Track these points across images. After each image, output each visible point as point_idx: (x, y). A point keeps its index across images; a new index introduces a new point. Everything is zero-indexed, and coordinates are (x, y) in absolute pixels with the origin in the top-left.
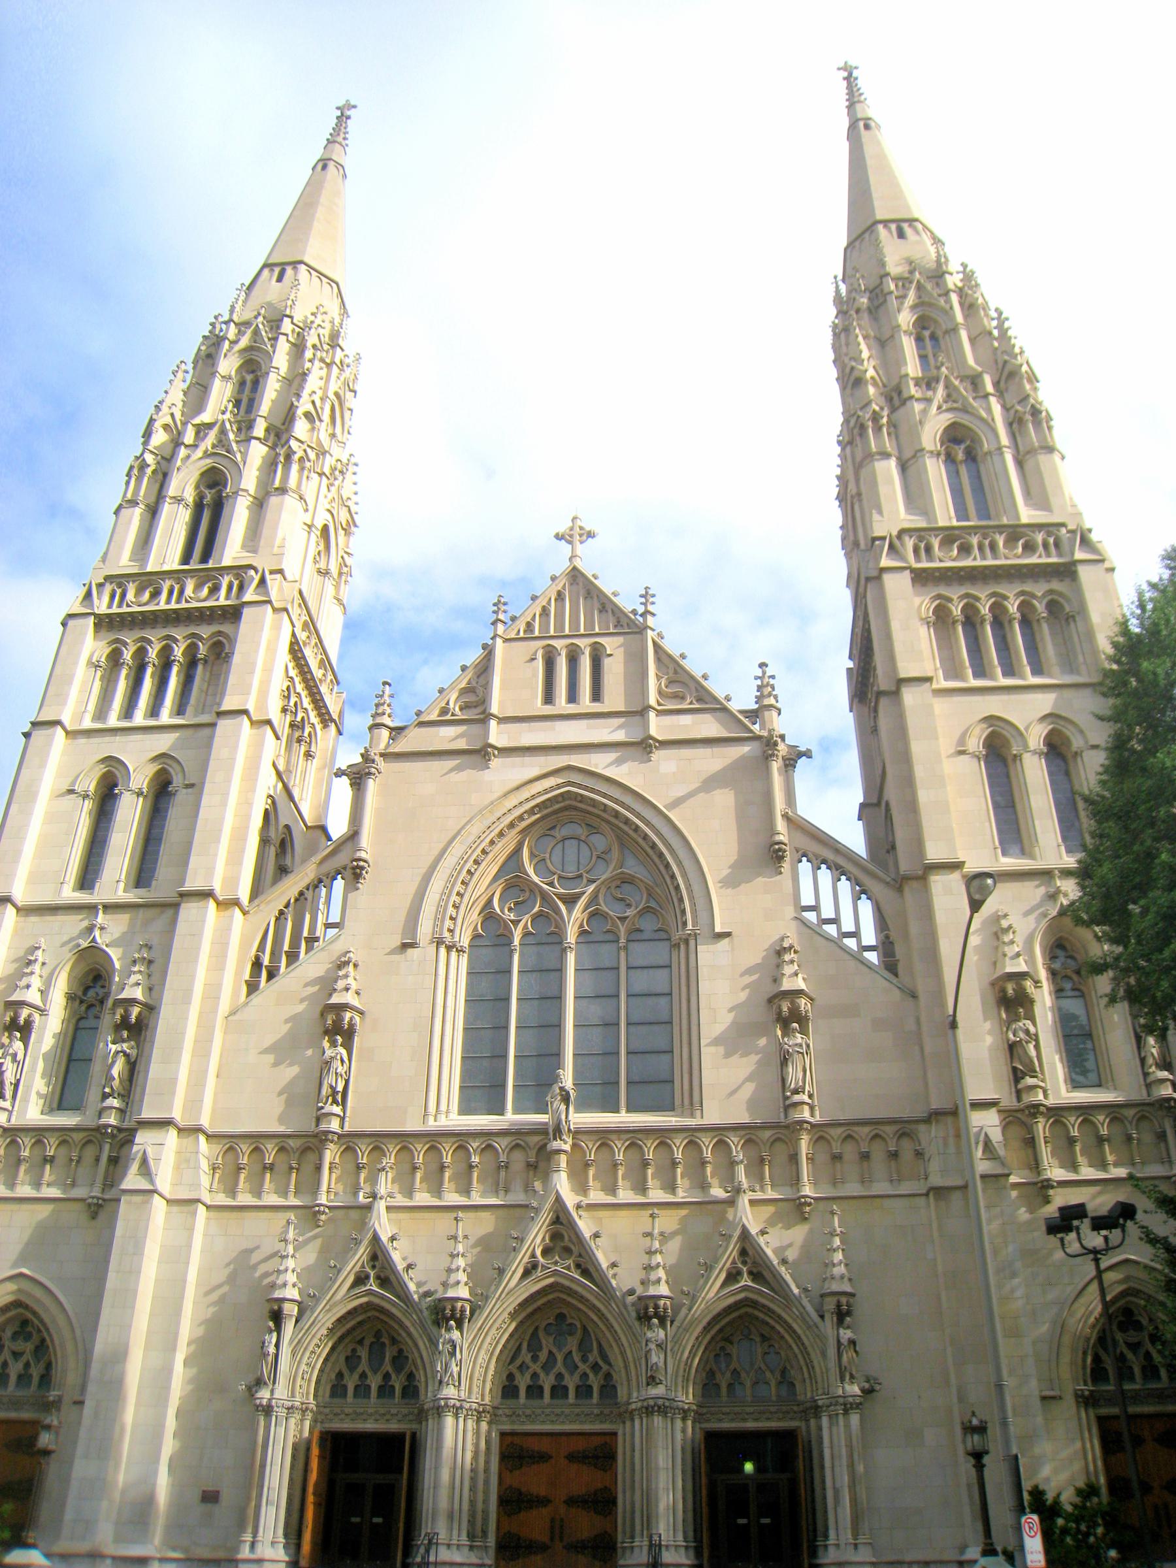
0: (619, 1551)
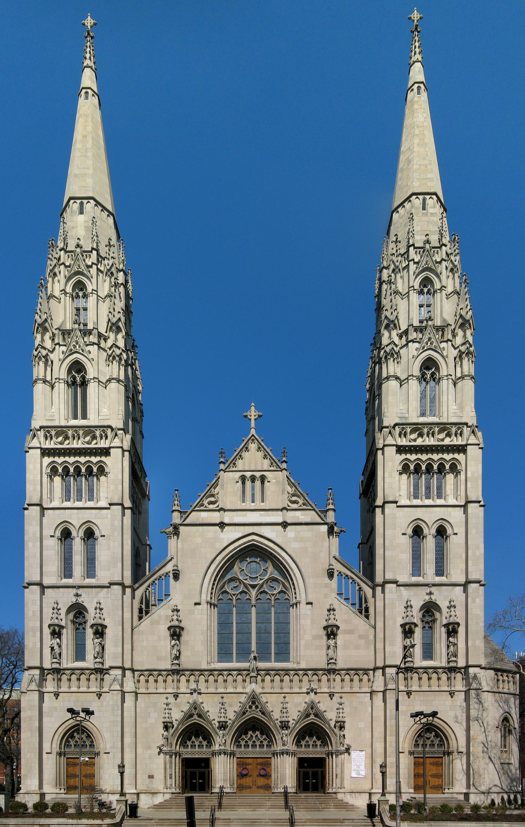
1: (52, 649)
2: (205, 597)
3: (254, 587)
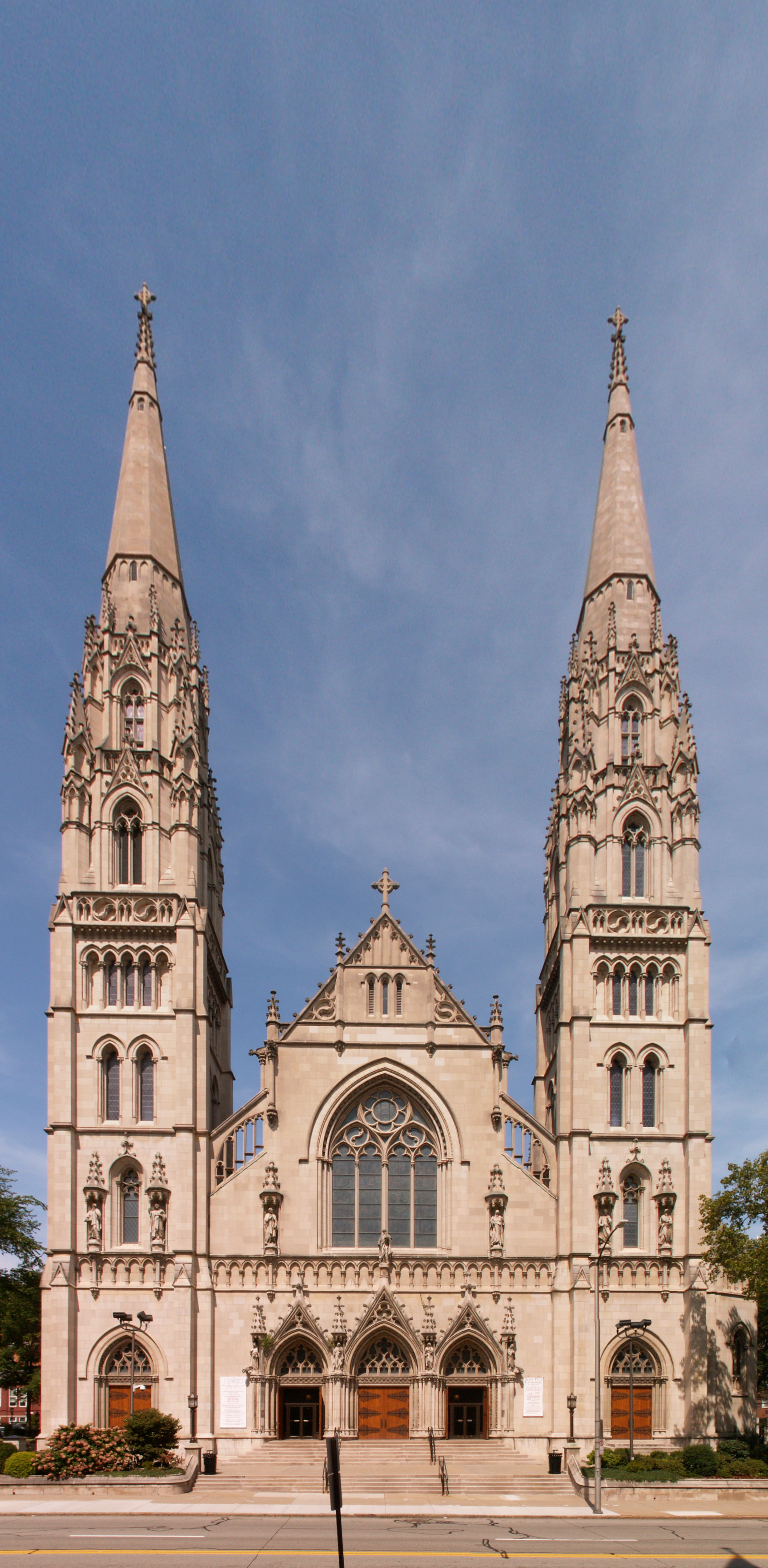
1: (89, 1223)
2: (315, 1151)
3: (385, 1137)
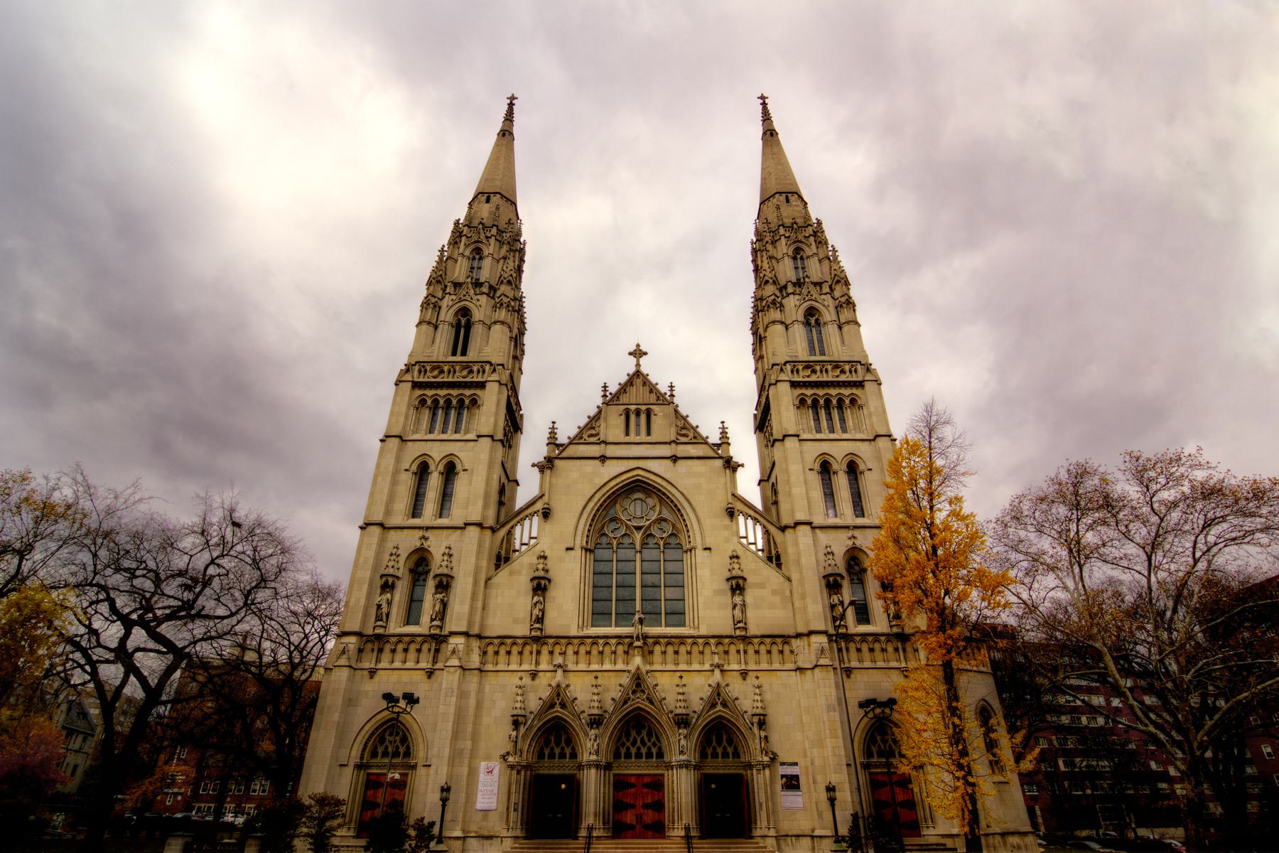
0: (667, 829)
1: (379, 606)
2: (580, 541)
